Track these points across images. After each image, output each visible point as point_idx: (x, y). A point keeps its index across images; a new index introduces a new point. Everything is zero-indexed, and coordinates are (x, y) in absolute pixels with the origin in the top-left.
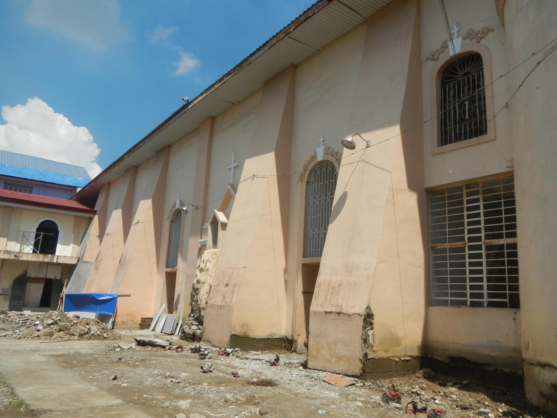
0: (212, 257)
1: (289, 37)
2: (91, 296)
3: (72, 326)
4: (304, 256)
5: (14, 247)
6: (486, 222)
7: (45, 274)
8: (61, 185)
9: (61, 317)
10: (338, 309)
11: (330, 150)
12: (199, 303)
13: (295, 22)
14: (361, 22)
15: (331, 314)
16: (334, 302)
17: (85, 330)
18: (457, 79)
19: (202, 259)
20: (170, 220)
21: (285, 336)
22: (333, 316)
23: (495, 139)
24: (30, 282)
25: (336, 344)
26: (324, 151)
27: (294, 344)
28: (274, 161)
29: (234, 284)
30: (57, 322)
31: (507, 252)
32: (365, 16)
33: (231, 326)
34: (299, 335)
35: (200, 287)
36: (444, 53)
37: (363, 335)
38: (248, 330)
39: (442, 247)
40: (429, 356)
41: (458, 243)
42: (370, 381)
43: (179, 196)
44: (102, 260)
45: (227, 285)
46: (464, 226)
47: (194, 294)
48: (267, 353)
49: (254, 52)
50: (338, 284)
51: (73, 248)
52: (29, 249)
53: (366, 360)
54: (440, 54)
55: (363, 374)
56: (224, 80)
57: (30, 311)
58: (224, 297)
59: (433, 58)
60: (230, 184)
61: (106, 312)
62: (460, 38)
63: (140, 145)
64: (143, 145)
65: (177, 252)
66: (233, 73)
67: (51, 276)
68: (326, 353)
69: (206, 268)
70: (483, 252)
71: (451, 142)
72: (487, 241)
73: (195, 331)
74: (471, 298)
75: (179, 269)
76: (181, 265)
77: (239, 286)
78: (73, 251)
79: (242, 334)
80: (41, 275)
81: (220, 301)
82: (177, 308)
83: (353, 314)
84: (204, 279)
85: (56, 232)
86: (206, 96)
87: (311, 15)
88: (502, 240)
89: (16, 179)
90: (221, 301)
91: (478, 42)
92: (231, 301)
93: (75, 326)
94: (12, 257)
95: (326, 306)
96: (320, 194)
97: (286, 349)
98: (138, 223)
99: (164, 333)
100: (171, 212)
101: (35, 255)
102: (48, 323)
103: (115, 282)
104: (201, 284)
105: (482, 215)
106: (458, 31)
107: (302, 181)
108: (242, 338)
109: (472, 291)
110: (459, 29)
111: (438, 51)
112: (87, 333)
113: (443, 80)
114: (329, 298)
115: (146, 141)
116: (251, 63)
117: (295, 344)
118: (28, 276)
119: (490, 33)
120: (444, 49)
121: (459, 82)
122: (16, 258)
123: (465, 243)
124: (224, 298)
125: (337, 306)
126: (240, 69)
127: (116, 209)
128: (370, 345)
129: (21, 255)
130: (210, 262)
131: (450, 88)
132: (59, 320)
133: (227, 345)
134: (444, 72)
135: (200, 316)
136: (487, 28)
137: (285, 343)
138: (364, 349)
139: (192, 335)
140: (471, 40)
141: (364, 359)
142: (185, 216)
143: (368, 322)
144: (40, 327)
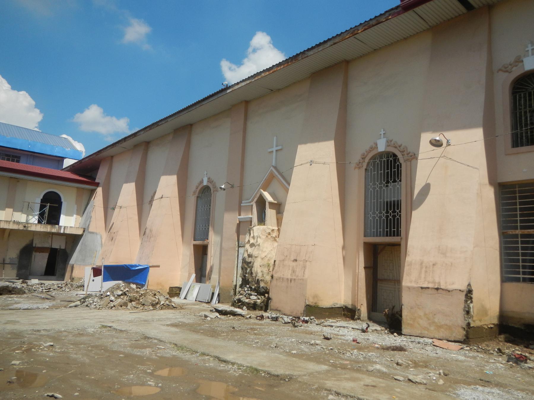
0: (262, 233)
1: (354, 37)
2: (126, 267)
3: (140, 296)
4: (365, 236)
5: (22, 217)
7: (51, 244)
8: (50, 155)
9: (128, 288)
11: (392, 143)
12: (254, 275)
13: (364, 25)
14: (425, 29)
15: (427, 289)
17: (155, 300)
18: (529, 90)
19: (252, 235)
20: (197, 195)
21: (344, 305)
22: (430, 291)
24: (36, 252)
25: (435, 315)
26: (386, 143)
27: (357, 312)
28: (334, 149)
29: (304, 260)
30: (126, 293)
32: (431, 24)
33: (306, 297)
34: (362, 305)
35: (252, 261)
37: (465, 307)
38: (318, 300)
39: (514, 233)
40: (504, 323)
41: (529, 230)
42: (474, 346)
43: (206, 174)
44: (117, 231)
45: (296, 260)
47: (246, 267)
48: (341, 320)
49: (312, 47)
50: (431, 264)
51: (76, 219)
52: (34, 220)
53: (469, 328)
54: (512, 68)
55: (467, 340)
56: (273, 70)
57: (38, 280)
58: (294, 271)
59: (506, 70)
60: (273, 166)
61: (138, 281)
63: (160, 123)
64: (165, 123)
65: (209, 226)
66: (285, 64)
67: (56, 246)
68: (423, 322)
69: (258, 243)
71: (522, 145)
73: (255, 300)
75: (212, 243)
76: (213, 240)
77: (311, 262)
78: (76, 221)
79: (314, 304)
80: (47, 245)
82: (210, 278)
83: (454, 290)
84: (256, 254)
85: (60, 204)
86: (250, 83)
87: (384, 20)
89: (4, 148)
90: (291, 274)
92: (303, 275)
93: (143, 296)
94: (21, 227)
95: (421, 282)
96: (381, 181)
97: (345, 316)
98: (162, 198)
99: (199, 301)
100: (197, 188)
101: (40, 225)
102: (118, 294)
103: (142, 254)
104: (253, 258)
108: (314, 308)
112: (157, 303)
114: (423, 276)
115: (169, 120)
116: (307, 56)
117: (358, 313)
118: (34, 245)
122: (25, 229)
124: (294, 272)
126: (294, 61)
127: (127, 182)
128: (472, 316)
129: (29, 225)
130: (260, 237)
131: (520, 98)
132: (127, 291)
133: (302, 314)
135: (259, 287)
137: (344, 312)
138: (467, 319)
139: (253, 304)
141: (467, 328)
143: (468, 296)
144: (112, 298)
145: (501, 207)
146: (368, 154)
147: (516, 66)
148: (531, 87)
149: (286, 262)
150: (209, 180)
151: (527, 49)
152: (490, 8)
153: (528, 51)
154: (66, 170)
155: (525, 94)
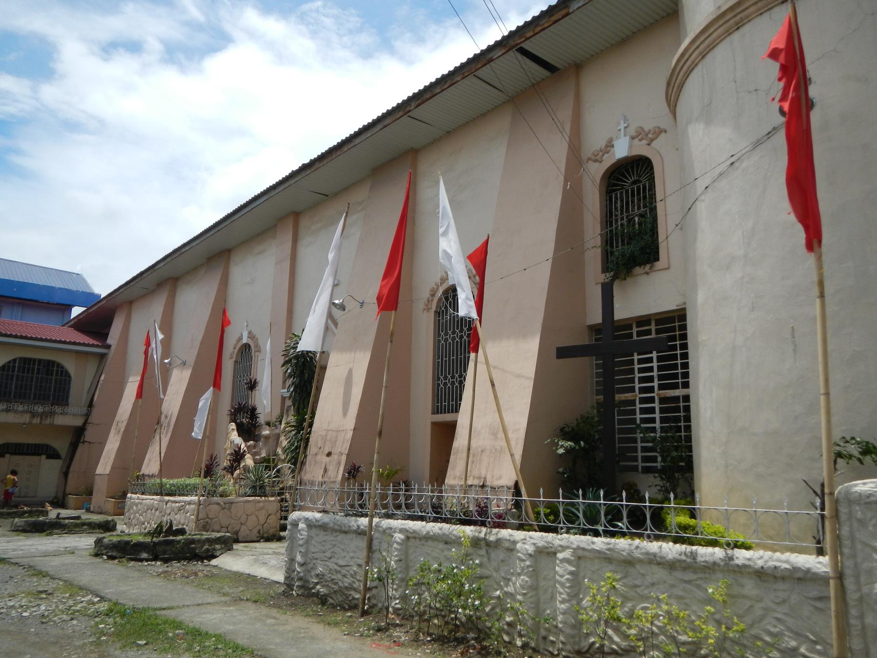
1: (408, 116)
4: (433, 413)
6: (660, 368)
10: (481, 481)
16: (476, 473)
20: (234, 359)
23: (668, 268)
29: (340, 452)
31: (683, 406)
32: (510, 95)
36: (609, 154)
41: (627, 395)
43: (247, 326)
46: (634, 373)
50: (480, 450)
54: (603, 155)
58: (326, 470)
62: (628, 138)
70: (657, 405)
72: (661, 392)
74: (642, 462)
81: (321, 476)
88: (677, 391)
91: (649, 145)
100: (235, 348)
105: (655, 360)
106: (625, 128)
107: (428, 310)
109: (644, 454)
110: (626, 125)
111: (601, 151)
113: (608, 187)
119: (663, 134)
120: (608, 149)
121: (627, 191)
123: (636, 395)
125: (479, 478)
131: (616, 198)
134: (609, 178)
136: (659, 128)
140: (640, 140)
145: (595, 362)
146: (438, 288)
147: (608, 152)
148: (628, 183)
149: (319, 457)
150: (251, 336)
151: (619, 128)
152: (578, 67)
153: (620, 130)
154: (69, 325)
155: (621, 193)
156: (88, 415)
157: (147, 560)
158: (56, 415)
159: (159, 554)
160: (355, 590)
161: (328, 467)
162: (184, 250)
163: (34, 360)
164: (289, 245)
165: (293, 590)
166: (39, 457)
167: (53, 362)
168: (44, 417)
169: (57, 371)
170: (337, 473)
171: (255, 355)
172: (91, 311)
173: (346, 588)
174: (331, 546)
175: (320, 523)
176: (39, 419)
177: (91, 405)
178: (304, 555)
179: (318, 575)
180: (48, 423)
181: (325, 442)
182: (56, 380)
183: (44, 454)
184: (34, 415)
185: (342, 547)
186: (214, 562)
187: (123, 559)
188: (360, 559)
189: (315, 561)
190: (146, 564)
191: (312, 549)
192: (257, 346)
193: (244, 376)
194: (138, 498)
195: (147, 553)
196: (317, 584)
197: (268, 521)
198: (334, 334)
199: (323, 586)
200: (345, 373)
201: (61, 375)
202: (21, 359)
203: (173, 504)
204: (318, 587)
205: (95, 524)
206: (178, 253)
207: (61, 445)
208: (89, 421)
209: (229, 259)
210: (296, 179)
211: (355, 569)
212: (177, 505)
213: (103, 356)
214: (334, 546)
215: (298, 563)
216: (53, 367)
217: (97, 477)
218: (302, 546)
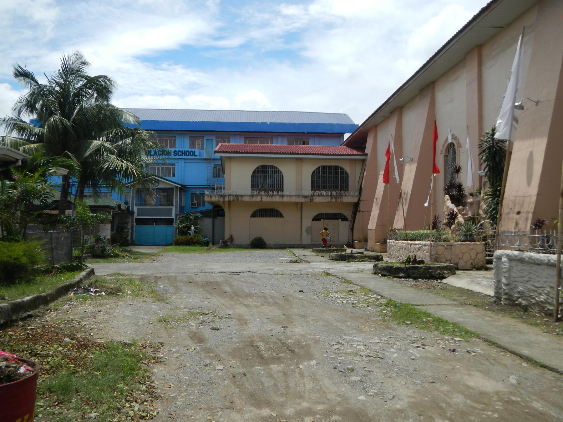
20: (444, 154)
43: (450, 131)
45: (519, 213)
81: (513, 228)
100: (443, 147)
142: (460, 150)
150: (454, 137)
156: (360, 196)
157: (404, 278)
158: (343, 197)
159: (410, 274)
160: (549, 304)
161: (518, 222)
162: (404, 88)
163: (329, 167)
164: (475, 70)
165: (501, 301)
166: (337, 220)
167: (338, 167)
168: (337, 198)
169: (341, 172)
170: (527, 226)
171: (457, 150)
172: (354, 135)
173: (542, 302)
174: (528, 274)
175: (518, 258)
176: (335, 200)
177: (360, 190)
178: (507, 278)
179: (519, 292)
180: (340, 201)
181: (515, 205)
182: (341, 177)
183: (340, 219)
184: (332, 197)
185: (537, 274)
186: (444, 281)
187: (390, 277)
188: (552, 283)
189: (516, 283)
190: (403, 280)
191: (513, 275)
192: (459, 143)
193: (451, 164)
194: (394, 242)
195: (404, 273)
196: (519, 298)
197: (477, 257)
198: (516, 129)
199: (524, 300)
200: (527, 155)
201: (343, 174)
202: (322, 166)
203: (415, 246)
204: (520, 300)
205: (372, 257)
206: (401, 90)
207: (348, 213)
208: (361, 199)
209: (434, 88)
210: (478, 21)
211: (548, 289)
212: (417, 246)
213: (364, 161)
214: (530, 273)
215: (504, 284)
216: (338, 169)
217: (369, 231)
218: (505, 272)
